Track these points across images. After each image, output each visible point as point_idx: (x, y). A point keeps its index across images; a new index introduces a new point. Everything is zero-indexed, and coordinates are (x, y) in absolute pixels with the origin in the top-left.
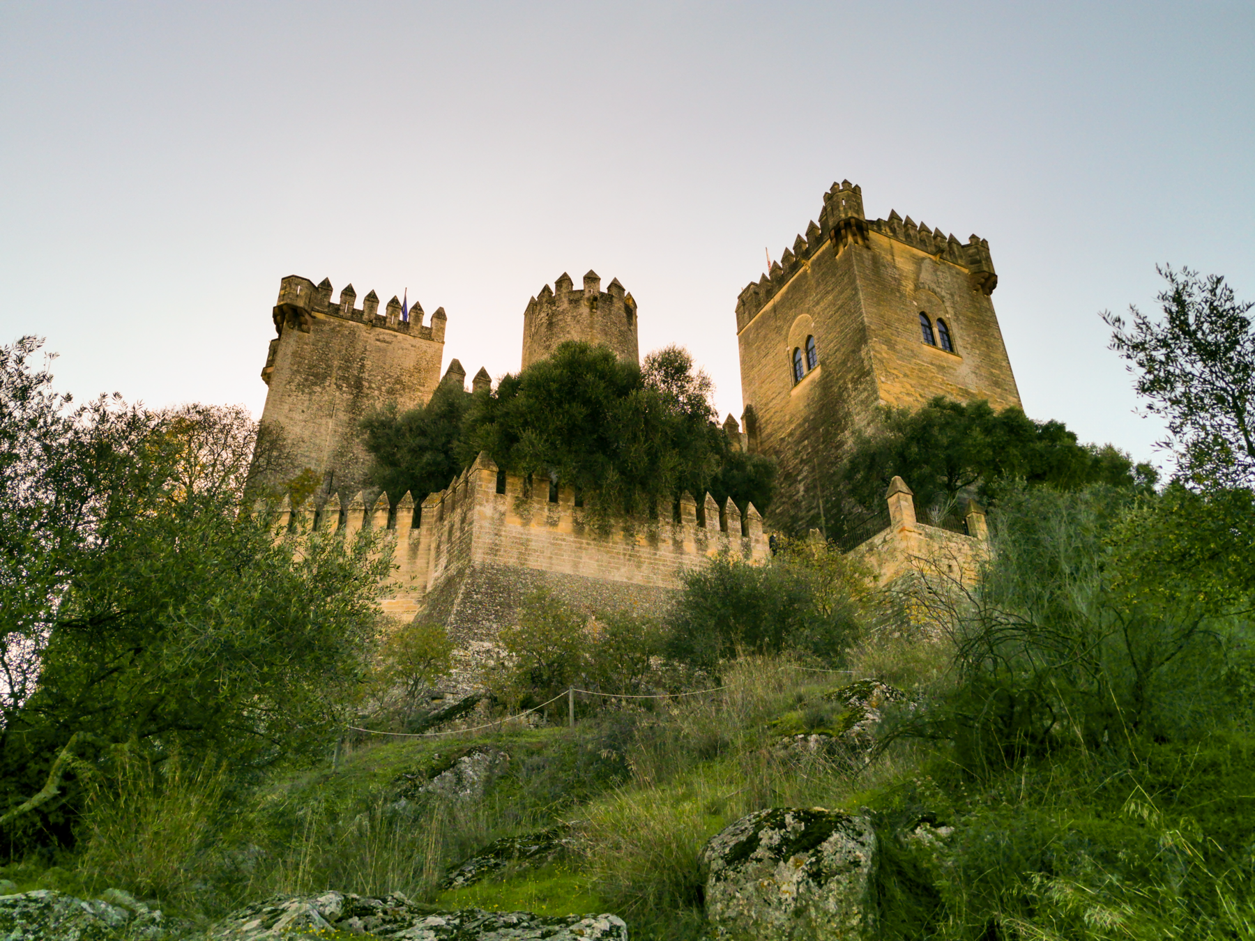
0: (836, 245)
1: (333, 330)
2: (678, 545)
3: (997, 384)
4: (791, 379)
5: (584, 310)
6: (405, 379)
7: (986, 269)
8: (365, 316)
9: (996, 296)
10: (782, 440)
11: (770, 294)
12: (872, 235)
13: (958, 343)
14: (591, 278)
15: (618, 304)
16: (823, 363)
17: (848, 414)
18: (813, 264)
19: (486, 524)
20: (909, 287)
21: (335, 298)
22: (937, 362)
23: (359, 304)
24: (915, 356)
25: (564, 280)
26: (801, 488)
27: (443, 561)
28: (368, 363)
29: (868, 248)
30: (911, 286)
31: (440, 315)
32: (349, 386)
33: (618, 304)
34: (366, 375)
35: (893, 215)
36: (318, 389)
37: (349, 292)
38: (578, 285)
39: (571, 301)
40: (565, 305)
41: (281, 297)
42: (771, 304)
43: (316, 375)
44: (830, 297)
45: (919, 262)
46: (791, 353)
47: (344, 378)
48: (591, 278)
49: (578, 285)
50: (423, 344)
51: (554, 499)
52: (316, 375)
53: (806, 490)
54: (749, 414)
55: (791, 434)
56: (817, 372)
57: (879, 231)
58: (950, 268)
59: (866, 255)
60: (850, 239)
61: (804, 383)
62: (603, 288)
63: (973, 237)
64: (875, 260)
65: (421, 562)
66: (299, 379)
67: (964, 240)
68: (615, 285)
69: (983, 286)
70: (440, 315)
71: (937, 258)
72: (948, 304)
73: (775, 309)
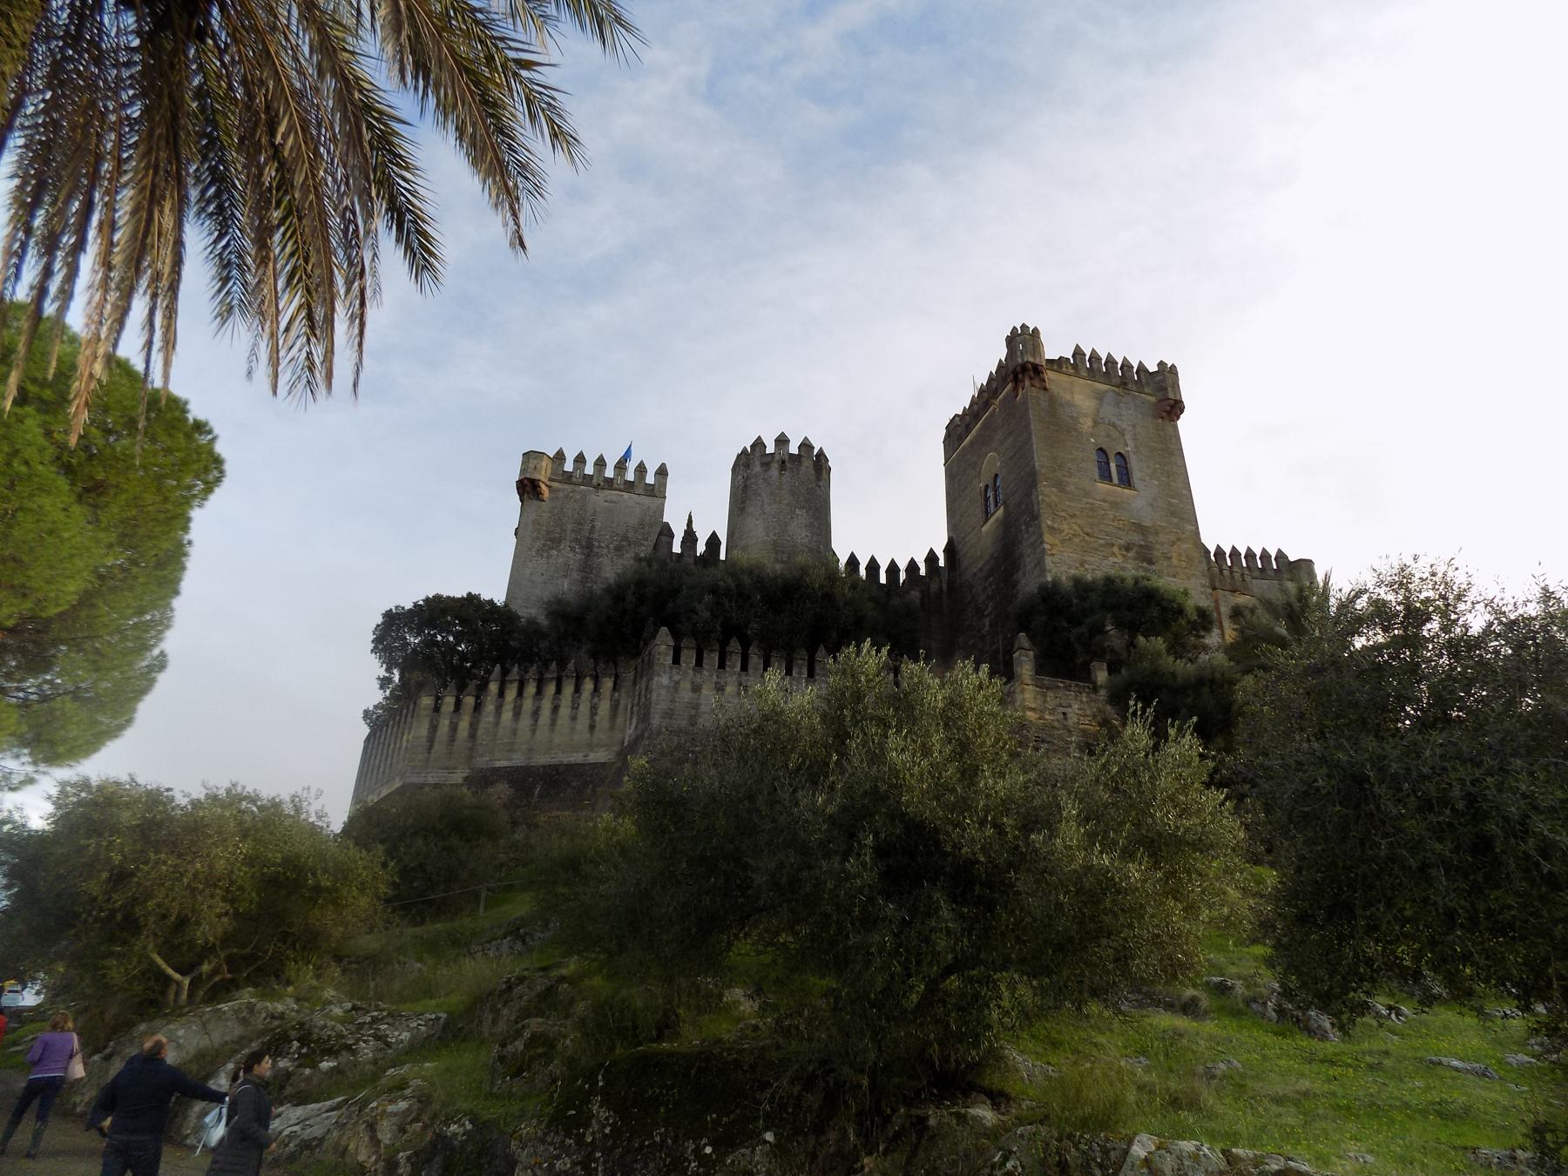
0: (1015, 389)
1: (566, 497)
3: (1174, 514)
5: (774, 471)
6: (630, 535)
7: (1171, 396)
8: (595, 481)
9: (1182, 423)
11: (968, 429)
12: (1050, 375)
13: (1136, 476)
14: (782, 441)
15: (807, 464)
16: (1004, 503)
17: (1021, 555)
19: (663, 692)
20: (1086, 424)
21: (569, 466)
23: (589, 469)
24: (1087, 494)
25: (759, 444)
26: (987, 622)
27: (634, 721)
28: (598, 524)
29: (1045, 389)
31: (662, 472)
32: (582, 547)
33: (807, 464)
35: (1078, 352)
37: (580, 459)
38: (770, 449)
39: (763, 464)
40: (757, 468)
41: (523, 471)
43: (552, 540)
45: (1100, 397)
47: (577, 540)
48: (782, 441)
49: (770, 449)
50: (646, 500)
51: (722, 665)
52: (552, 540)
53: (991, 625)
54: (950, 549)
55: (981, 570)
56: (1001, 510)
58: (1134, 398)
59: (1042, 396)
60: (1027, 383)
61: (992, 520)
62: (793, 449)
63: (1161, 364)
64: (1053, 400)
65: (619, 721)
66: (538, 544)
67: (1153, 368)
68: (806, 445)
69: (1169, 413)
70: (662, 472)
71: (1120, 390)
72: (1128, 437)
73: (972, 443)
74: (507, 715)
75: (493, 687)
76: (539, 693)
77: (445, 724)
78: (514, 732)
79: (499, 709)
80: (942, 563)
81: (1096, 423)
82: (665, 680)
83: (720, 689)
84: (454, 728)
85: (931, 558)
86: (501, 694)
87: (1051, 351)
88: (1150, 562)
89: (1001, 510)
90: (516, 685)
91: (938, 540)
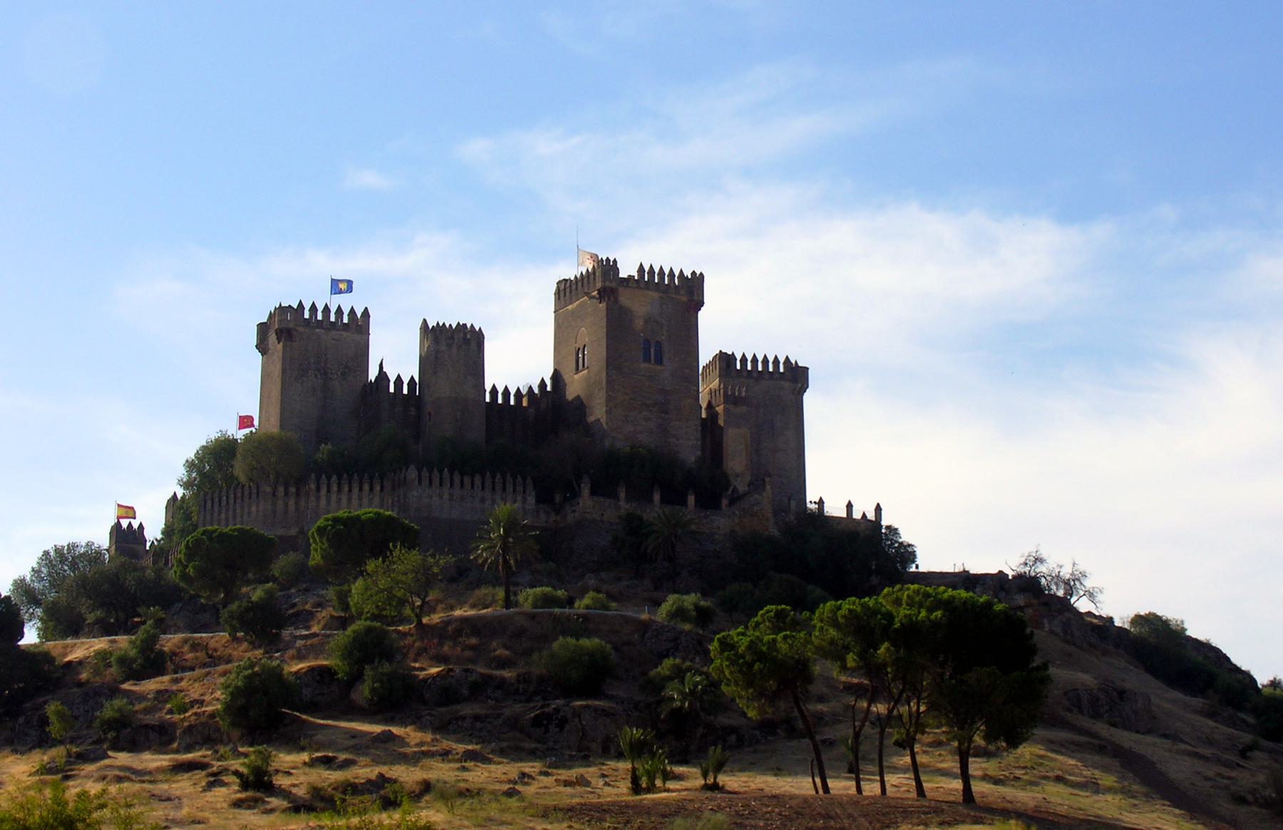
5: (454, 351)
9: (702, 314)
15: (473, 345)
31: (366, 313)
42: (570, 307)
50: (358, 337)
54: (556, 377)
57: (627, 286)
63: (694, 273)
67: (688, 273)
73: (573, 311)
75: (313, 486)
76: (339, 491)
77: (280, 504)
79: (318, 499)
80: (549, 389)
82: (415, 493)
83: (441, 497)
84: (286, 505)
85: (543, 384)
86: (318, 489)
87: (623, 274)
88: (666, 413)
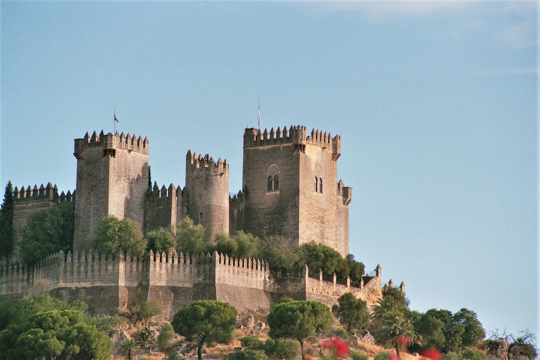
2: (252, 275)
4: (267, 188)
10: (259, 209)
16: (281, 191)
18: (284, 147)
20: (313, 166)
22: (316, 199)
28: (131, 168)
30: (314, 167)
34: (130, 174)
36: (120, 182)
44: (288, 167)
46: (268, 176)
47: (126, 176)
55: (263, 209)
66: (115, 179)
73: (263, 151)
74: (158, 268)
78: (160, 275)
79: (155, 266)
81: (316, 166)
86: (155, 260)
88: (323, 223)
89: (278, 192)
90: (159, 258)
91: (241, 188)
